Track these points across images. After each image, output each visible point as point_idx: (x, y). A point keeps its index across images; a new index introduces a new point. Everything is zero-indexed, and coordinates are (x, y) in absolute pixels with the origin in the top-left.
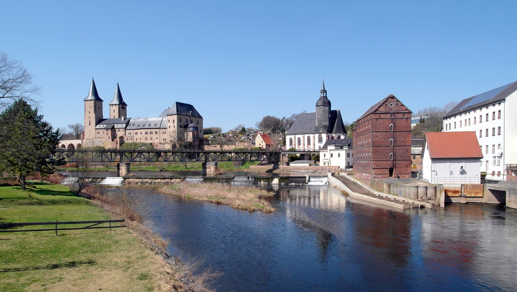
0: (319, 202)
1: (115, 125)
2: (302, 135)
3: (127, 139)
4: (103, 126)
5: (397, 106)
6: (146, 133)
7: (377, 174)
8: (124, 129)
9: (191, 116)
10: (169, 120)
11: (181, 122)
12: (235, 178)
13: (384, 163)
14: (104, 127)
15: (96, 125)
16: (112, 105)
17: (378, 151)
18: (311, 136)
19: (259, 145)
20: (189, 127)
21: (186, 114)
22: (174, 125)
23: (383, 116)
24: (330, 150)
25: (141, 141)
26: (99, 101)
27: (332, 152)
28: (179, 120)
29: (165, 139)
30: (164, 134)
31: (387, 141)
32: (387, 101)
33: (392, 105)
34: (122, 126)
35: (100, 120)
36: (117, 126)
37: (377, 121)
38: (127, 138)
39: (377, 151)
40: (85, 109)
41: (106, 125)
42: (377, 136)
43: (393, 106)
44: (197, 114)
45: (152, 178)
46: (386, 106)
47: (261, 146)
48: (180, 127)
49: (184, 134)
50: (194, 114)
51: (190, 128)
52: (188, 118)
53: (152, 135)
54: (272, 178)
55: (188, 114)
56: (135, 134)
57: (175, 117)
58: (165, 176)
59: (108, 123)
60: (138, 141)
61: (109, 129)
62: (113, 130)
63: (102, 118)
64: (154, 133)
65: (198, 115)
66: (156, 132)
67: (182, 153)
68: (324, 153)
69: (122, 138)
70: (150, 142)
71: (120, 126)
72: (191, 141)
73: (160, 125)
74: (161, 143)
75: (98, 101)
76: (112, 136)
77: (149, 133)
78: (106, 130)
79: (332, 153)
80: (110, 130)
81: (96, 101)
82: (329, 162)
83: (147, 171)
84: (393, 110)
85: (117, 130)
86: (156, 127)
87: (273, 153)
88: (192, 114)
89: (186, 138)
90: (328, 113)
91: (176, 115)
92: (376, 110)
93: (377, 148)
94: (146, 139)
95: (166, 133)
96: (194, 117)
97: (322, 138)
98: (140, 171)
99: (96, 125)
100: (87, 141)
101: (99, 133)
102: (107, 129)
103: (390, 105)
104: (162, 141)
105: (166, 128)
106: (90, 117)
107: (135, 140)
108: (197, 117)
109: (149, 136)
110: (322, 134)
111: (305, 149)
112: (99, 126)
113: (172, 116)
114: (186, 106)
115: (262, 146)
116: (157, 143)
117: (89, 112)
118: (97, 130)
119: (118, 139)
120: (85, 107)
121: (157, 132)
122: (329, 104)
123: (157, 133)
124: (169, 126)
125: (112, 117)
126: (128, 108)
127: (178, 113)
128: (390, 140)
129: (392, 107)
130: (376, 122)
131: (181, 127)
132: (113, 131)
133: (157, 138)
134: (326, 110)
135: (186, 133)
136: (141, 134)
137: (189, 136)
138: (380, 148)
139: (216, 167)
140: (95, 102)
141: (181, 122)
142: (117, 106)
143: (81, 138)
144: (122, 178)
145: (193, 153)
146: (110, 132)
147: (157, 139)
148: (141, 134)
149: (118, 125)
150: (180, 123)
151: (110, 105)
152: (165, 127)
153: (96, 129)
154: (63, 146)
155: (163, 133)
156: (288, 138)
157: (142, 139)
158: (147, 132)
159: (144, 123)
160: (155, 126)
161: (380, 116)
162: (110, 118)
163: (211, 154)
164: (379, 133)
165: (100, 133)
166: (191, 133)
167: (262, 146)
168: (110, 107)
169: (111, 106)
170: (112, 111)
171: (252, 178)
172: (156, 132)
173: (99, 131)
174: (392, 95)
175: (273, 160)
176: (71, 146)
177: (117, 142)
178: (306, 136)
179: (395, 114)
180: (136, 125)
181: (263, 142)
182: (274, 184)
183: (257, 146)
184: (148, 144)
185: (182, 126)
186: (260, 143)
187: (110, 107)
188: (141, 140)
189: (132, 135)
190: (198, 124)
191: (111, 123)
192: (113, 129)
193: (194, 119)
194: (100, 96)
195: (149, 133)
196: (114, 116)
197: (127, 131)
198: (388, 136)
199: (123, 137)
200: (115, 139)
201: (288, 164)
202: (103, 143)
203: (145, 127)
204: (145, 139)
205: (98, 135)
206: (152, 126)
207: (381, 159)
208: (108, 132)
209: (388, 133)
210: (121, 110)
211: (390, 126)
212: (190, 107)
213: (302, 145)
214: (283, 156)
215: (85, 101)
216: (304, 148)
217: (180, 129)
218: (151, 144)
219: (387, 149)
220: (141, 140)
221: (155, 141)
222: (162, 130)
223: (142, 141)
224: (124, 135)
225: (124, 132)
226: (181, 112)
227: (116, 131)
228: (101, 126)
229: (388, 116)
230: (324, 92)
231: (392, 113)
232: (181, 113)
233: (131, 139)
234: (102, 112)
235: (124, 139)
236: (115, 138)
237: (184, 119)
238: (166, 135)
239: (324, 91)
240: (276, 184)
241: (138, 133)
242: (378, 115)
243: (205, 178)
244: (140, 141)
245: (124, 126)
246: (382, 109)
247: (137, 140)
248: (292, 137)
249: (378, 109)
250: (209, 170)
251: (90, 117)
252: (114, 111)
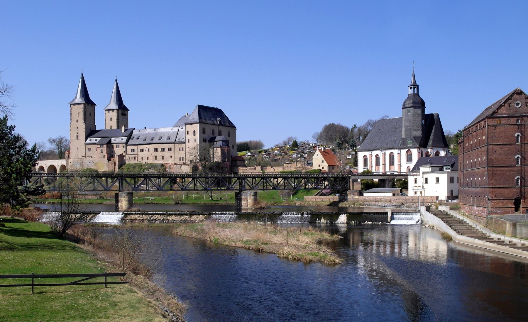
0: (407, 250)
1: (112, 138)
2: (381, 150)
3: (129, 159)
4: (96, 140)
5: (526, 106)
6: (156, 150)
7: (496, 208)
8: (124, 145)
9: (218, 125)
10: (188, 131)
11: (205, 134)
12: (283, 214)
13: (506, 191)
14: (97, 141)
15: (86, 139)
16: (109, 110)
17: (497, 173)
18: (396, 152)
19: (318, 166)
20: (217, 141)
21: (212, 122)
22: (195, 137)
23: (504, 121)
24: (424, 173)
25: (148, 161)
26: (90, 105)
27: (426, 176)
28: (203, 131)
29: (183, 158)
30: (181, 152)
31: (511, 158)
32: (511, 99)
33: (518, 104)
34: (122, 140)
35: (91, 132)
36: (115, 140)
37: (495, 129)
38: (129, 157)
39: (496, 174)
40: (71, 117)
41: (100, 139)
42: (496, 152)
43: (520, 106)
44: (227, 122)
45: (164, 214)
46: (509, 106)
47: (321, 168)
48: (204, 141)
49: (209, 151)
50: (223, 122)
51: (218, 142)
52: (216, 128)
53: (163, 153)
54: (337, 214)
55: (215, 122)
56: (139, 151)
57: (197, 127)
58: (182, 212)
59: (102, 136)
60: (144, 162)
62: (109, 145)
63: (94, 129)
64: (167, 149)
65: (229, 123)
66: (169, 148)
67: (207, 178)
68: (415, 177)
69: (121, 157)
70: (161, 162)
71: (119, 140)
72: (220, 161)
73: (175, 138)
74: (177, 164)
75: (88, 105)
76: (107, 154)
77: (159, 150)
78: (99, 146)
79: (426, 177)
80: (106, 146)
81: (87, 105)
82: (422, 190)
83: (157, 203)
84: (520, 112)
85: (115, 145)
86: (169, 141)
87: (338, 178)
88: (220, 122)
89: (212, 156)
90: (420, 118)
91: (198, 124)
92: (494, 113)
93: (495, 169)
94: (156, 158)
95: (184, 149)
96: (224, 126)
97: (411, 155)
98: (146, 203)
99: (86, 139)
100: (73, 161)
101: (89, 150)
102: (101, 144)
103: (515, 104)
104: (178, 161)
105: (184, 143)
106: (77, 128)
107: (140, 160)
108: (228, 126)
109: (159, 154)
110: (412, 150)
111: (386, 171)
112: (91, 140)
113: (192, 125)
114: (213, 110)
115: (323, 168)
116: (170, 164)
117: (77, 120)
118: (87, 146)
119: (116, 159)
120: (71, 114)
121: (171, 148)
122: (422, 104)
123: (171, 150)
124: (188, 140)
125: (108, 128)
126: (129, 113)
127: (201, 121)
128: (516, 157)
129: (518, 107)
130: (495, 131)
131: (205, 140)
132: (110, 147)
133: (171, 157)
134: (418, 114)
135: (212, 150)
136: (149, 151)
137: (217, 154)
138: (499, 169)
139: (255, 198)
140: (84, 107)
141: (205, 134)
142: (116, 111)
143: (66, 157)
144: (122, 213)
145: (222, 178)
146: (105, 148)
147: (171, 158)
148: (149, 151)
149: (117, 138)
150: (203, 135)
151: (105, 110)
152: (183, 141)
153: (86, 144)
154: (42, 168)
155: (180, 150)
156: (361, 155)
157: (150, 158)
158: (157, 149)
159: (153, 136)
160: (168, 139)
161: (500, 121)
162: (105, 128)
163: (247, 180)
164: (498, 147)
165: (91, 150)
166: (219, 150)
167: (323, 168)
168: (105, 114)
169: (107, 112)
170: (108, 119)
171: (307, 214)
172: (169, 148)
173: (89, 147)
174: (519, 90)
175: (338, 187)
176: (52, 168)
177: (115, 163)
178: (388, 152)
179: (523, 118)
180: (142, 138)
181: (325, 161)
182: (341, 223)
183: (315, 167)
184: (158, 166)
185: (206, 140)
186: (319, 164)
187: (105, 114)
188: (148, 159)
189: (136, 152)
190: (229, 136)
191: (107, 136)
192: (109, 144)
193: (224, 130)
194: (92, 98)
195: (159, 150)
196: (111, 126)
197: (128, 147)
198: (512, 150)
199: (124, 156)
200: (112, 159)
201: (361, 194)
202: (96, 164)
203: (154, 141)
204: (154, 159)
205: (89, 153)
206: (164, 140)
207: (502, 186)
208: (102, 148)
209: (513, 146)
210: (121, 117)
211: (516, 135)
212: (217, 113)
213: (381, 166)
214: (353, 182)
215: (71, 104)
216: (385, 170)
217: (204, 143)
218: (162, 165)
219: (510, 171)
220: (148, 159)
221: (168, 161)
222: (178, 146)
223: (150, 161)
224: (125, 153)
225: (124, 149)
226: (205, 120)
227: (113, 148)
228: (93, 140)
229: (513, 121)
230: (414, 88)
231: (519, 117)
232: (205, 121)
233: (135, 159)
234: (95, 120)
235: (125, 158)
236: (113, 156)
237: (209, 129)
238: (184, 152)
239: (415, 86)
240: (343, 223)
241: (144, 150)
242: (497, 119)
243: (239, 214)
244: (147, 161)
245: (125, 139)
246: (503, 111)
247: (142, 160)
248: (367, 153)
249: (496, 111)
250: (245, 202)
251: (77, 128)
252: (111, 118)
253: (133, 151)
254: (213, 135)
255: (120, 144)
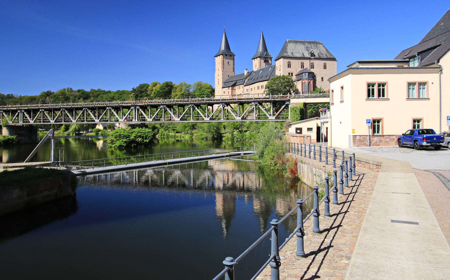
1: (238, 81)
6: (258, 87)
61: (229, 87)
78: (227, 88)
149: (239, 81)
169: (254, 60)
170: (254, 66)
185: (292, 73)
195: (260, 87)
208: (229, 90)
227: (237, 89)
253: (247, 90)
254: (302, 68)
255: (240, 86)
